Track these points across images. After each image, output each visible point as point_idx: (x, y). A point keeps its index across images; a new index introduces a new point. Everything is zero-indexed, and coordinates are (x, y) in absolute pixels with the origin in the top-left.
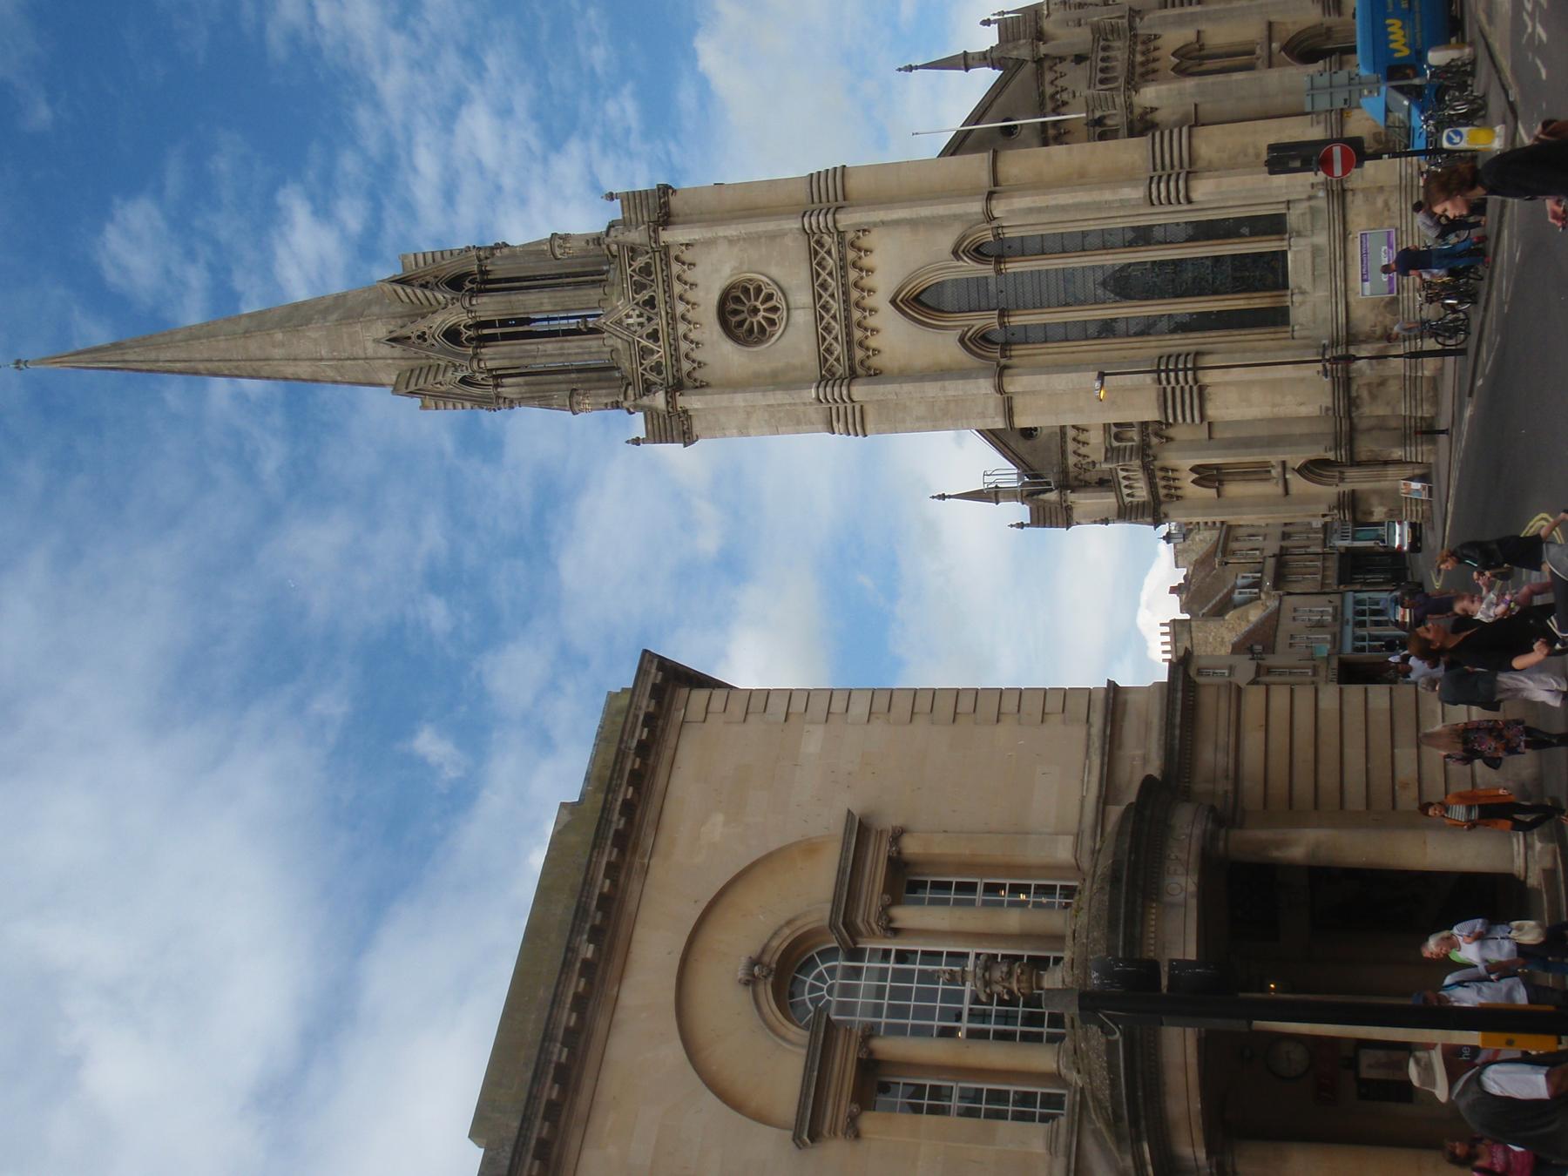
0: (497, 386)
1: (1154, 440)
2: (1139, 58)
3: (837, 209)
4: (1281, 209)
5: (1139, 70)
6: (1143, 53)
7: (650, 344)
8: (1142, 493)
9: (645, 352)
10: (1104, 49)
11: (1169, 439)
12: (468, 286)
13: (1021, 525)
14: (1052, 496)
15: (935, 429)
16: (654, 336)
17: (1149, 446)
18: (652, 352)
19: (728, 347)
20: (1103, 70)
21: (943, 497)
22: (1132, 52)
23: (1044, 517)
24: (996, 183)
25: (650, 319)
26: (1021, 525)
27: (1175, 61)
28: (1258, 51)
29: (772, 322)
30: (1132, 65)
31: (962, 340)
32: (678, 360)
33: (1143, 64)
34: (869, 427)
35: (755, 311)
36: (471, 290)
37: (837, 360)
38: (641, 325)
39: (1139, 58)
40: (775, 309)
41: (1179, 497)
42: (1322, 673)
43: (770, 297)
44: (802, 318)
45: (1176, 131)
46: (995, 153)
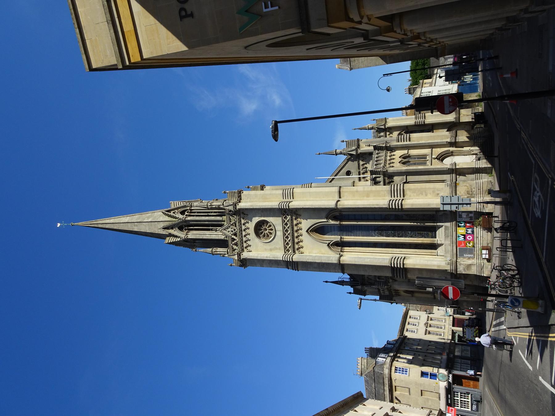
0: (195, 242)
1: (391, 281)
2: (388, 158)
3: (290, 202)
4: (434, 213)
5: (388, 162)
6: (390, 156)
7: (234, 237)
8: (387, 293)
9: (234, 240)
10: (377, 154)
11: (396, 281)
12: (186, 213)
13: (350, 293)
14: (359, 287)
15: (319, 271)
16: (235, 234)
17: (389, 282)
18: (235, 240)
19: (257, 240)
20: (376, 161)
21: (327, 282)
22: (386, 156)
23: (356, 292)
24: (340, 197)
25: (235, 230)
26: (350, 293)
27: (400, 159)
28: (428, 158)
29: (271, 233)
30: (386, 160)
31: (328, 245)
32: (242, 243)
33: (390, 160)
34: (299, 269)
35: (266, 230)
36: (186, 215)
37: (290, 247)
38: (232, 231)
39: (388, 158)
40: (272, 230)
41: (399, 295)
42: (447, 322)
43: (270, 226)
44: (280, 234)
45: (399, 185)
46: (340, 187)
